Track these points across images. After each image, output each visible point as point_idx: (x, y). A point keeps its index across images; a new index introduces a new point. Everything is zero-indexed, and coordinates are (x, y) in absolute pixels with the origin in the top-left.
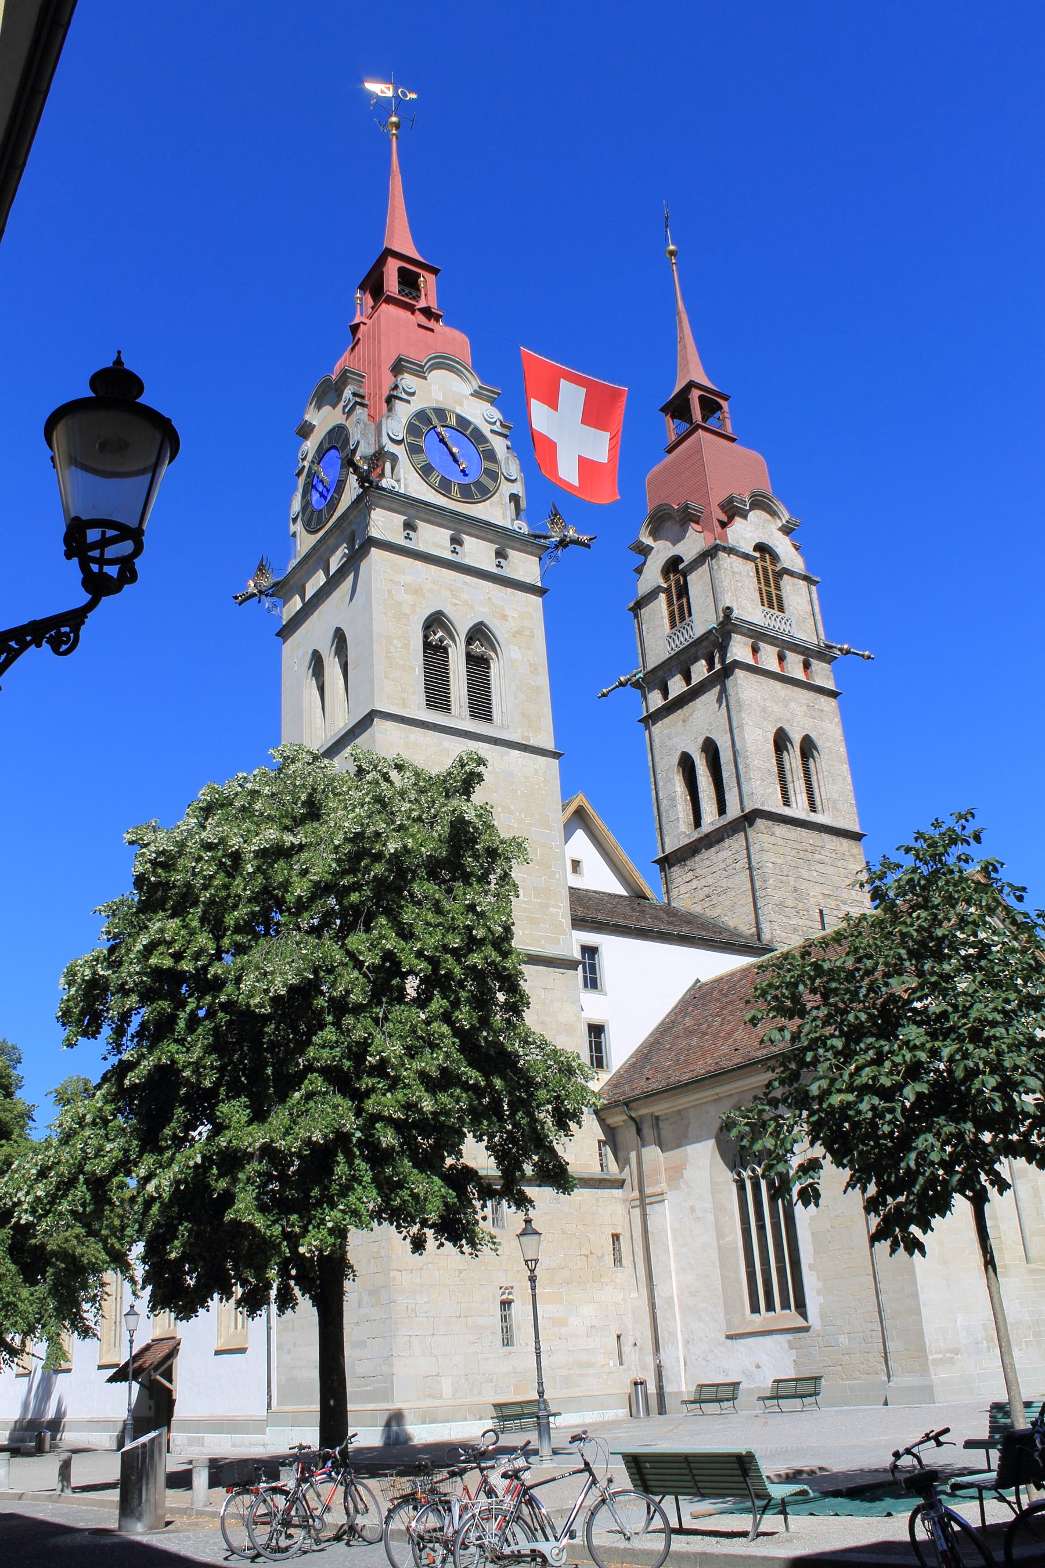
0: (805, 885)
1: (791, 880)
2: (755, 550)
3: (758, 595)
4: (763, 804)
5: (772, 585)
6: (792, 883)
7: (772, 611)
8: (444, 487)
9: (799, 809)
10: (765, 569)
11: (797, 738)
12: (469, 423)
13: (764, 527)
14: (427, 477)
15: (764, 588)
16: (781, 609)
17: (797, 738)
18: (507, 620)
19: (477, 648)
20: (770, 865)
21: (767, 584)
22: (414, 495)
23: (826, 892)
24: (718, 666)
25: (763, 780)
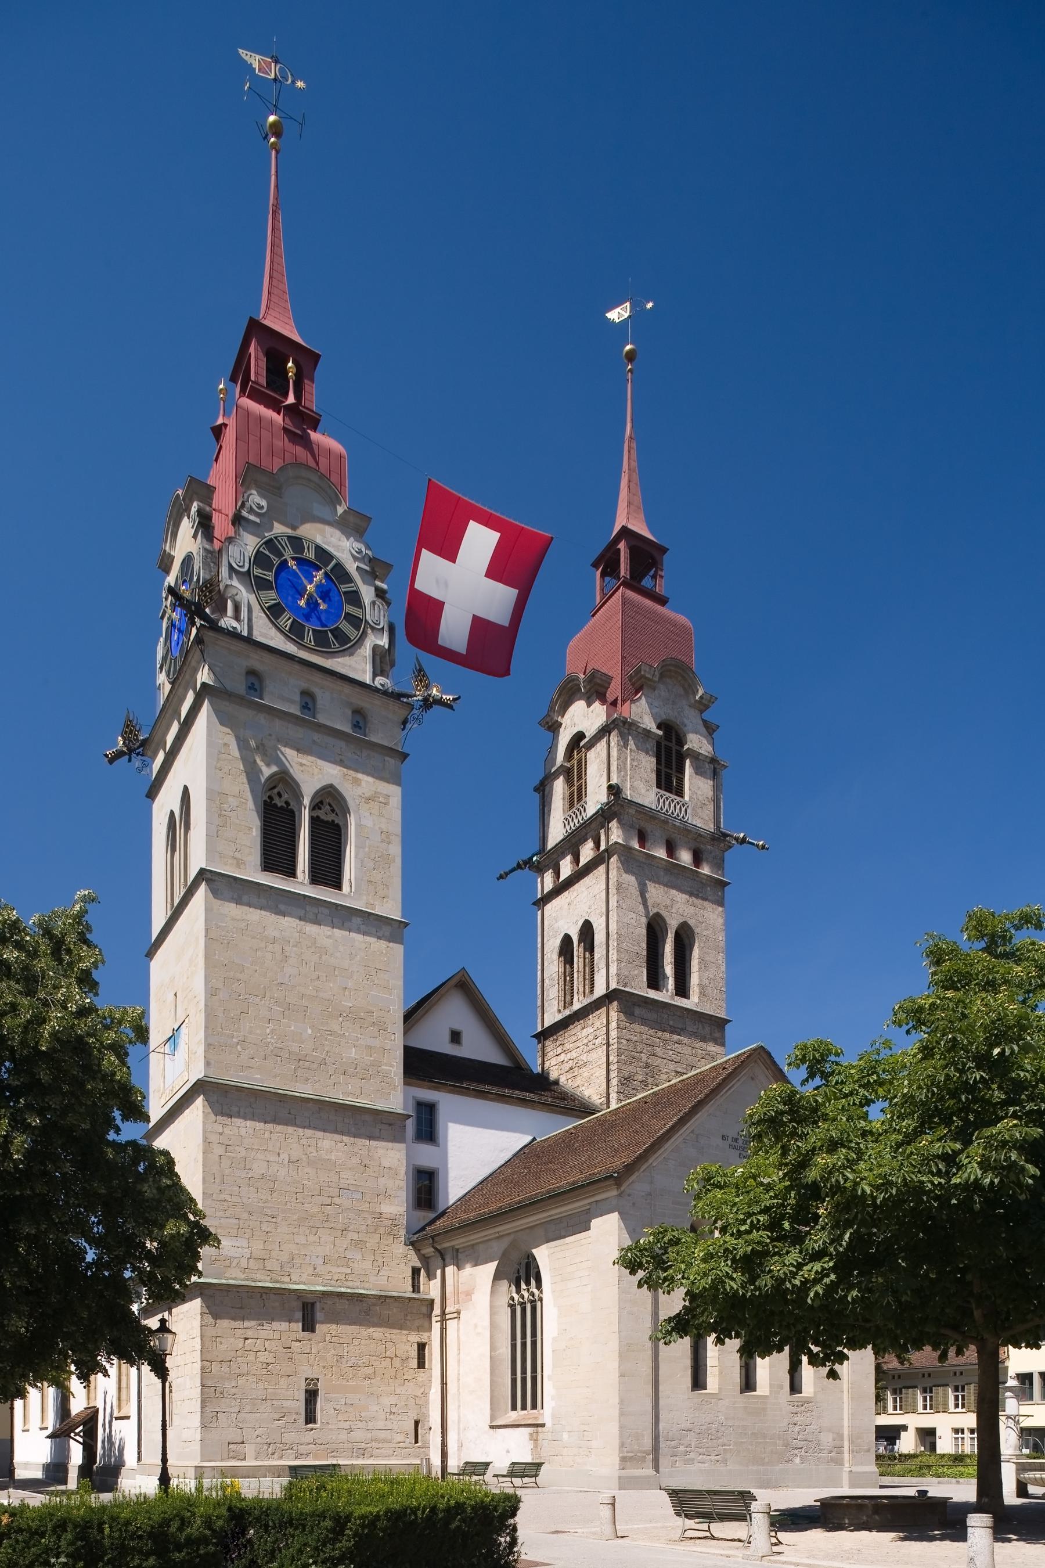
0: (658, 1062)
1: (644, 1057)
2: (659, 727)
3: (654, 776)
4: (625, 985)
5: (674, 767)
6: (644, 1059)
7: (668, 794)
8: (295, 633)
9: (666, 995)
10: (668, 750)
11: (673, 924)
12: (329, 557)
13: (674, 703)
14: (277, 618)
15: (663, 769)
16: (680, 793)
17: (673, 924)
18: (359, 785)
19: (324, 815)
20: (625, 1042)
21: (668, 765)
22: (259, 639)
23: (679, 1070)
24: (603, 847)
25: (629, 963)
